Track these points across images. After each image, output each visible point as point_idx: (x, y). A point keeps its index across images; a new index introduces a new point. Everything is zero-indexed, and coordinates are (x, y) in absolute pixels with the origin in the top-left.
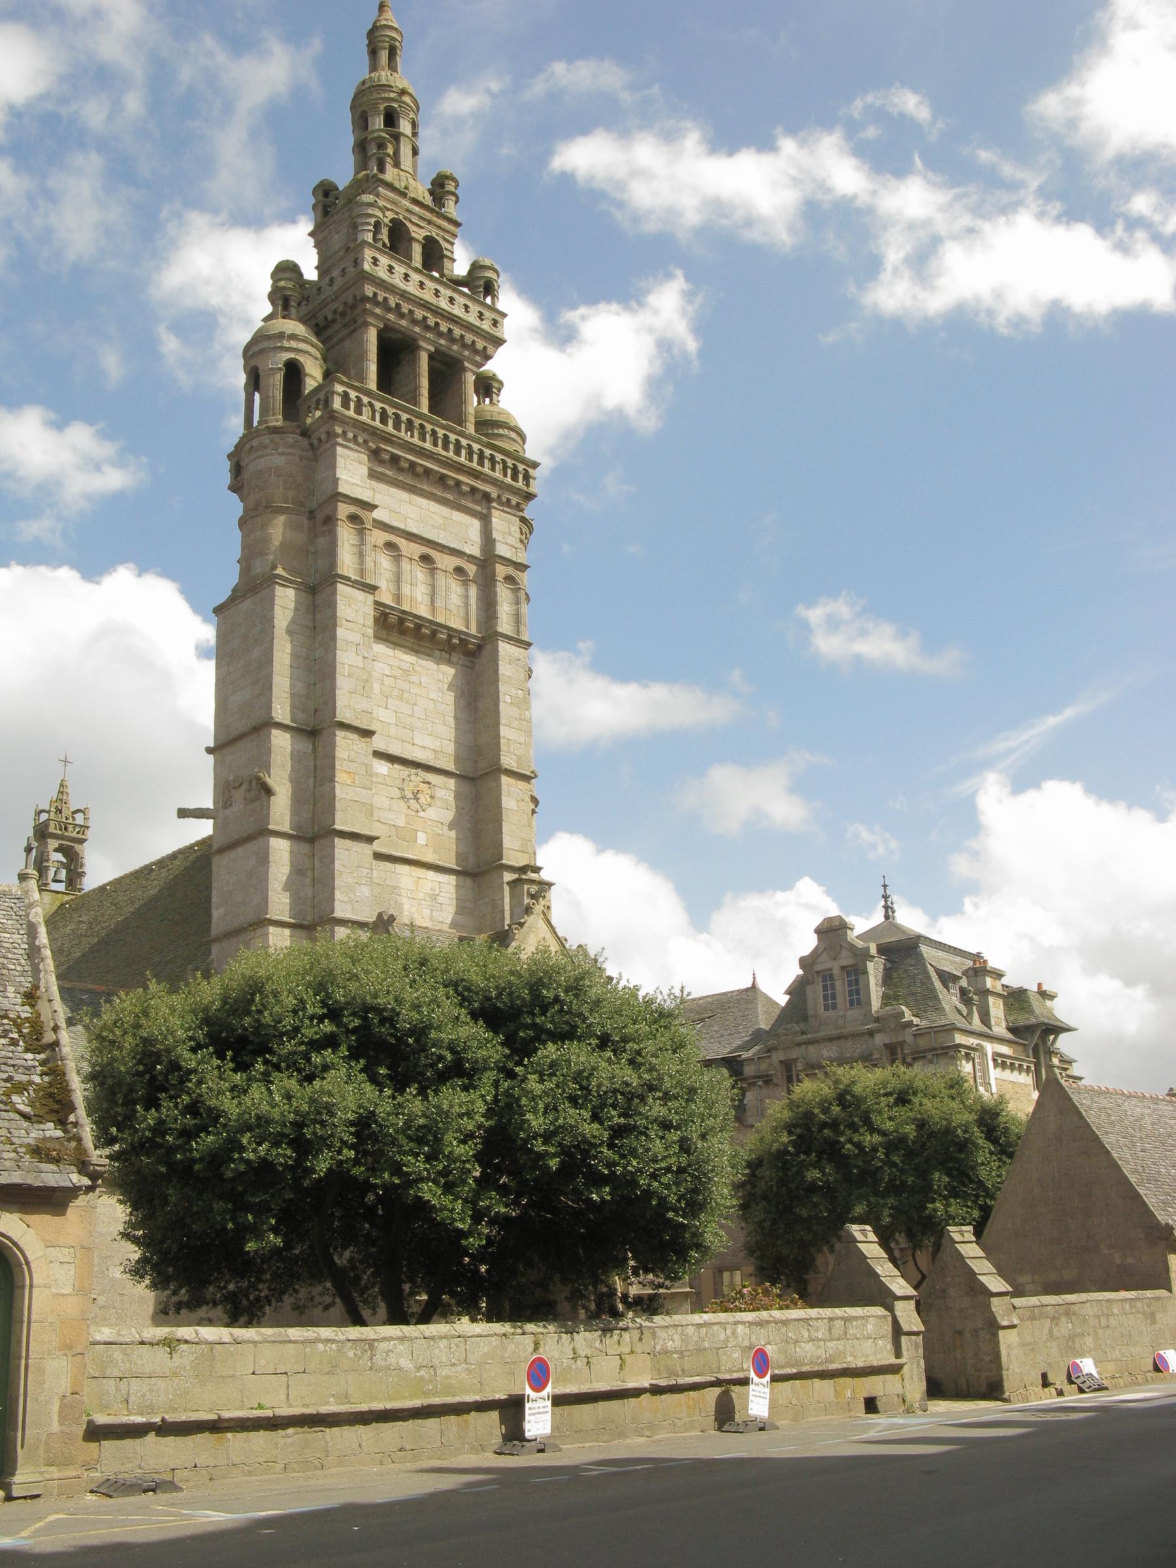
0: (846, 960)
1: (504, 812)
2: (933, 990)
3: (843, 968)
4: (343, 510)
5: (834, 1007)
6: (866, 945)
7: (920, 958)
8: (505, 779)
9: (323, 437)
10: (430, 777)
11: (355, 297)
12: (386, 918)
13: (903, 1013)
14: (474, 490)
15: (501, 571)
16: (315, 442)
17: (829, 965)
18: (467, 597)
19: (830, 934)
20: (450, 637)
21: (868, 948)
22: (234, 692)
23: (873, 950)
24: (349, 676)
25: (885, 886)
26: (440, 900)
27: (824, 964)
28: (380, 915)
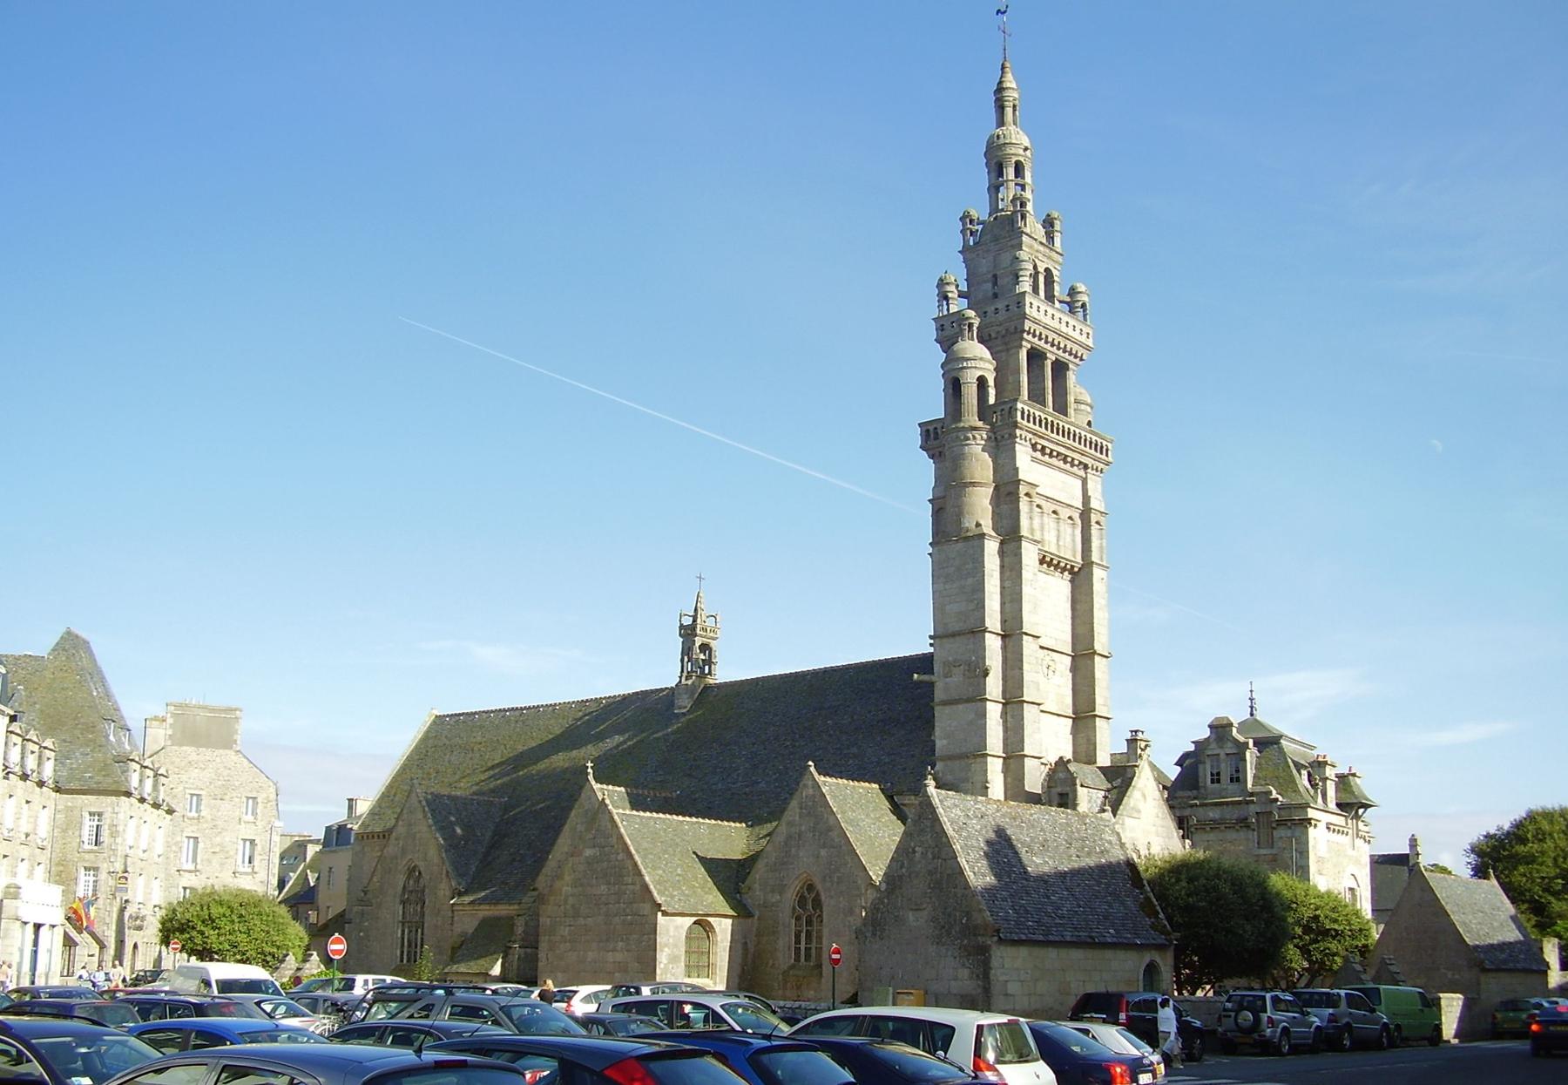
0: (1229, 748)
2: (1292, 776)
3: (1227, 754)
4: (1023, 489)
5: (1219, 781)
6: (1246, 740)
7: (1281, 750)
8: (1097, 658)
9: (1006, 436)
11: (1016, 328)
13: (1271, 792)
14: (1080, 463)
15: (1094, 518)
16: (999, 437)
17: (1215, 752)
18: (1073, 535)
19: (1220, 729)
20: (1066, 564)
21: (1248, 743)
23: (1251, 742)
25: (1251, 691)
27: (1214, 749)
28: (1061, 758)
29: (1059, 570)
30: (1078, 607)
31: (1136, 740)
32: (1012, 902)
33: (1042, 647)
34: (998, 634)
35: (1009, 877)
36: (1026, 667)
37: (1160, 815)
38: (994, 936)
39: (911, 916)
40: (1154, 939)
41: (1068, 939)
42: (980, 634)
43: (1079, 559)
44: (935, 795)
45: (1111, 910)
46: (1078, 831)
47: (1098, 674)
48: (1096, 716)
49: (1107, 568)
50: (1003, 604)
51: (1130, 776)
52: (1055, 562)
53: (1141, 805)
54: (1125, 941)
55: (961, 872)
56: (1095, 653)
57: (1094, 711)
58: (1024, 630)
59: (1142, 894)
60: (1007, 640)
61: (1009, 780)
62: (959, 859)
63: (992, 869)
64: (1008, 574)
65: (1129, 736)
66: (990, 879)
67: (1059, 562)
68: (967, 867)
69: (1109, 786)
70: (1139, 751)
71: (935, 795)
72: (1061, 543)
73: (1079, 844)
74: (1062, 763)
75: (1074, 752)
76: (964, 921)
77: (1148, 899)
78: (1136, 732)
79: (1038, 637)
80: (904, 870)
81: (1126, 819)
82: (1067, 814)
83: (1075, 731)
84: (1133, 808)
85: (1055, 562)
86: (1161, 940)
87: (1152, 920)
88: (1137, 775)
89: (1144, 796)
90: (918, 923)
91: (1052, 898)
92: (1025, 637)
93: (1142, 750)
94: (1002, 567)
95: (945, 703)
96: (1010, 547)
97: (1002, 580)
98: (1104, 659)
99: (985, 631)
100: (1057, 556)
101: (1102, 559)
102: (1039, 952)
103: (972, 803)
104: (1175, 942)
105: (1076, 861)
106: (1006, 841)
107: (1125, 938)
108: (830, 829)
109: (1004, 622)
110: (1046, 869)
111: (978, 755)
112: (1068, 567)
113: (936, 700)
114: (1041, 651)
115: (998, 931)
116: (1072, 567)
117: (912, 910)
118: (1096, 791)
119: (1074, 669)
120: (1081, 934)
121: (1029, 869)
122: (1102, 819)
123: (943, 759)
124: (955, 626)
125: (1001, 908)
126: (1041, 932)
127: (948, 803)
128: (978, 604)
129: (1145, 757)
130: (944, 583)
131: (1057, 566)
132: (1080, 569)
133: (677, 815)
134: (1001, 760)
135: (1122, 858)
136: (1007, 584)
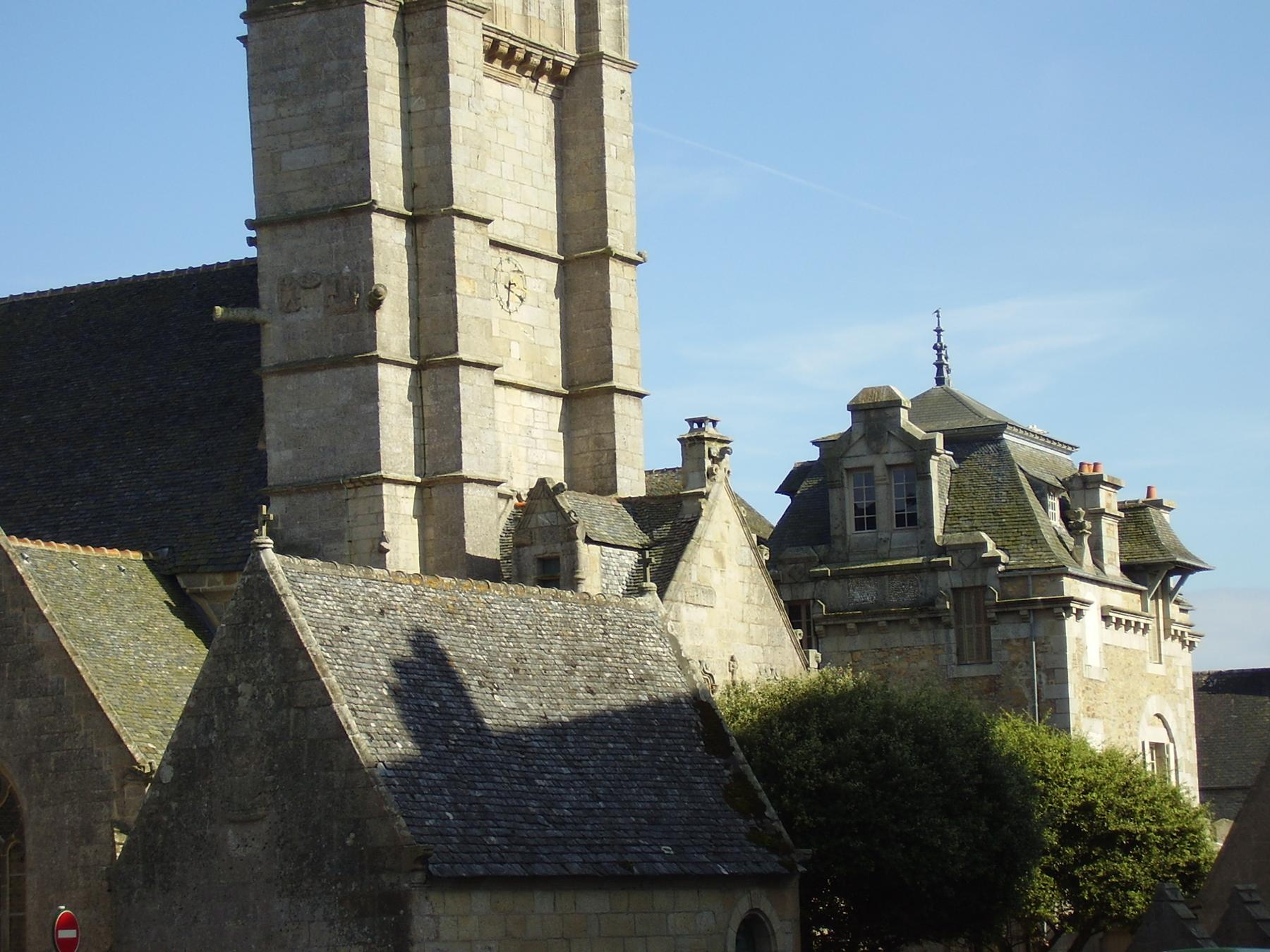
0: (894, 454)
1: (613, 314)
2: (1028, 510)
3: (890, 467)
5: (872, 524)
6: (930, 436)
7: (1003, 455)
8: (614, 267)
10: (523, 261)
12: (551, 486)
13: (984, 544)
17: (866, 461)
19: (872, 414)
20: (544, 60)
21: (934, 441)
22: (292, 147)
23: (940, 444)
24: (464, 143)
25: (939, 331)
26: (535, 433)
27: (860, 456)
28: (542, 482)
29: (529, 73)
30: (571, 154)
31: (701, 440)
32: (453, 795)
33: (495, 244)
34: (398, 216)
35: (445, 739)
36: (462, 287)
37: (755, 599)
38: (415, 870)
39: (231, 836)
40: (758, 863)
41: (575, 869)
42: (360, 216)
43: (570, 48)
44: (279, 568)
45: (663, 805)
46: (590, 636)
47: (616, 300)
48: (615, 390)
49: (634, 67)
50: (408, 149)
51: (688, 516)
52: (520, 55)
53: (715, 579)
54: (697, 871)
55: (340, 733)
56: (608, 254)
57: (611, 379)
58: (454, 207)
59: (727, 767)
60: (419, 227)
61: (431, 532)
62: (335, 705)
63: (408, 724)
64: (416, 82)
65: (685, 430)
66: (404, 746)
67: (528, 55)
68: (353, 722)
69: (646, 539)
70: (708, 463)
71: (279, 568)
72: (532, 13)
73: (591, 665)
74: (543, 492)
75: (569, 469)
76: (349, 842)
77: (740, 777)
78: (700, 421)
79: (488, 221)
80: (213, 736)
81: (683, 608)
82: (565, 602)
83: (569, 425)
84: (697, 586)
85: (520, 55)
86: (772, 864)
87: (752, 822)
88: (704, 513)
89: (720, 558)
90: (249, 850)
91: (537, 781)
92: (458, 222)
93: (715, 460)
94: (405, 66)
95: (285, 369)
96: (420, 22)
97: (405, 96)
98: (629, 269)
99: (371, 208)
100: (522, 41)
101: (620, 48)
102: (507, 900)
103: (359, 582)
104: (801, 869)
105: (585, 701)
106: (435, 661)
107: (696, 863)
108: (35, 655)
109: (411, 188)
110: (523, 720)
111: (360, 480)
112: (549, 65)
113: (267, 362)
114: (492, 251)
115: (424, 860)
116: (558, 65)
117: (233, 822)
118: (618, 551)
119: (565, 290)
120: (601, 857)
121: (486, 720)
122: (639, 610)
123: (287, 490)
124: (306, 200)
125: (429, 810)
126: (518, 858)
127: (309, 584)
128: (352, 150)
129: (720, 474)
130: (278, 104)
131: (523, 65)
132: (573, 70)
133: (110, 548)
134: (413, 489)
135: (684, 690)
136: (417, 104)
